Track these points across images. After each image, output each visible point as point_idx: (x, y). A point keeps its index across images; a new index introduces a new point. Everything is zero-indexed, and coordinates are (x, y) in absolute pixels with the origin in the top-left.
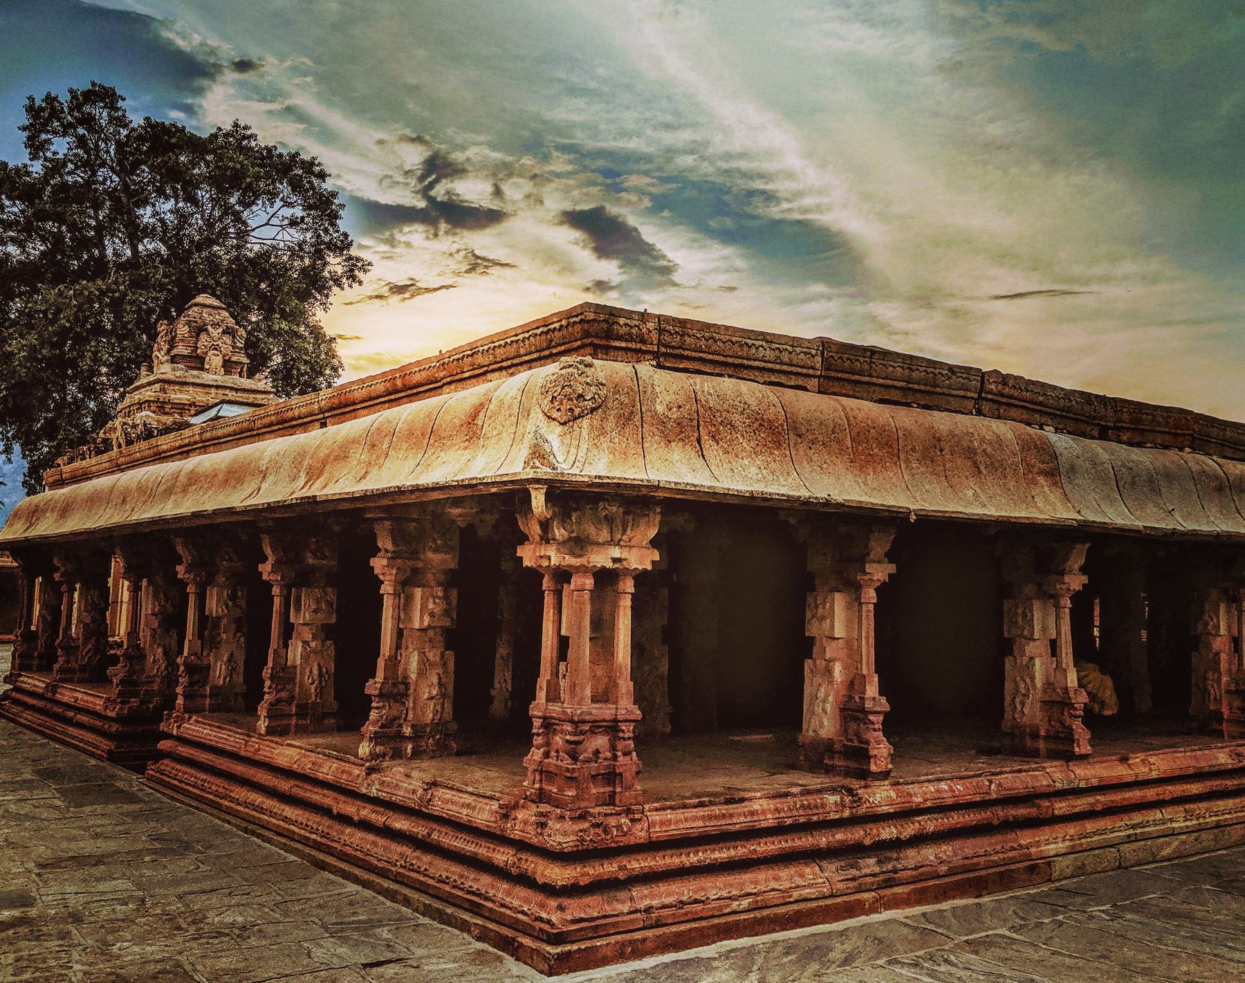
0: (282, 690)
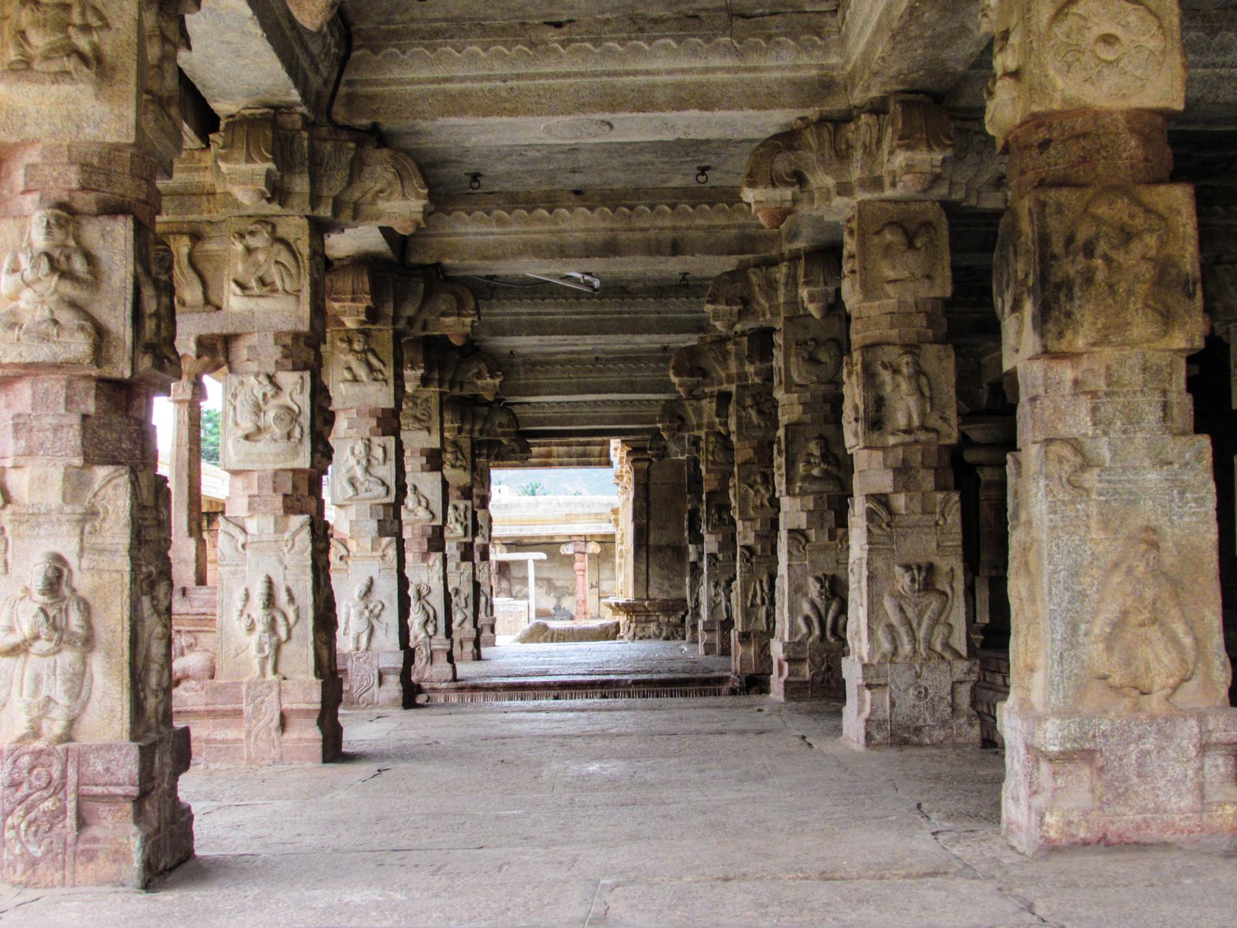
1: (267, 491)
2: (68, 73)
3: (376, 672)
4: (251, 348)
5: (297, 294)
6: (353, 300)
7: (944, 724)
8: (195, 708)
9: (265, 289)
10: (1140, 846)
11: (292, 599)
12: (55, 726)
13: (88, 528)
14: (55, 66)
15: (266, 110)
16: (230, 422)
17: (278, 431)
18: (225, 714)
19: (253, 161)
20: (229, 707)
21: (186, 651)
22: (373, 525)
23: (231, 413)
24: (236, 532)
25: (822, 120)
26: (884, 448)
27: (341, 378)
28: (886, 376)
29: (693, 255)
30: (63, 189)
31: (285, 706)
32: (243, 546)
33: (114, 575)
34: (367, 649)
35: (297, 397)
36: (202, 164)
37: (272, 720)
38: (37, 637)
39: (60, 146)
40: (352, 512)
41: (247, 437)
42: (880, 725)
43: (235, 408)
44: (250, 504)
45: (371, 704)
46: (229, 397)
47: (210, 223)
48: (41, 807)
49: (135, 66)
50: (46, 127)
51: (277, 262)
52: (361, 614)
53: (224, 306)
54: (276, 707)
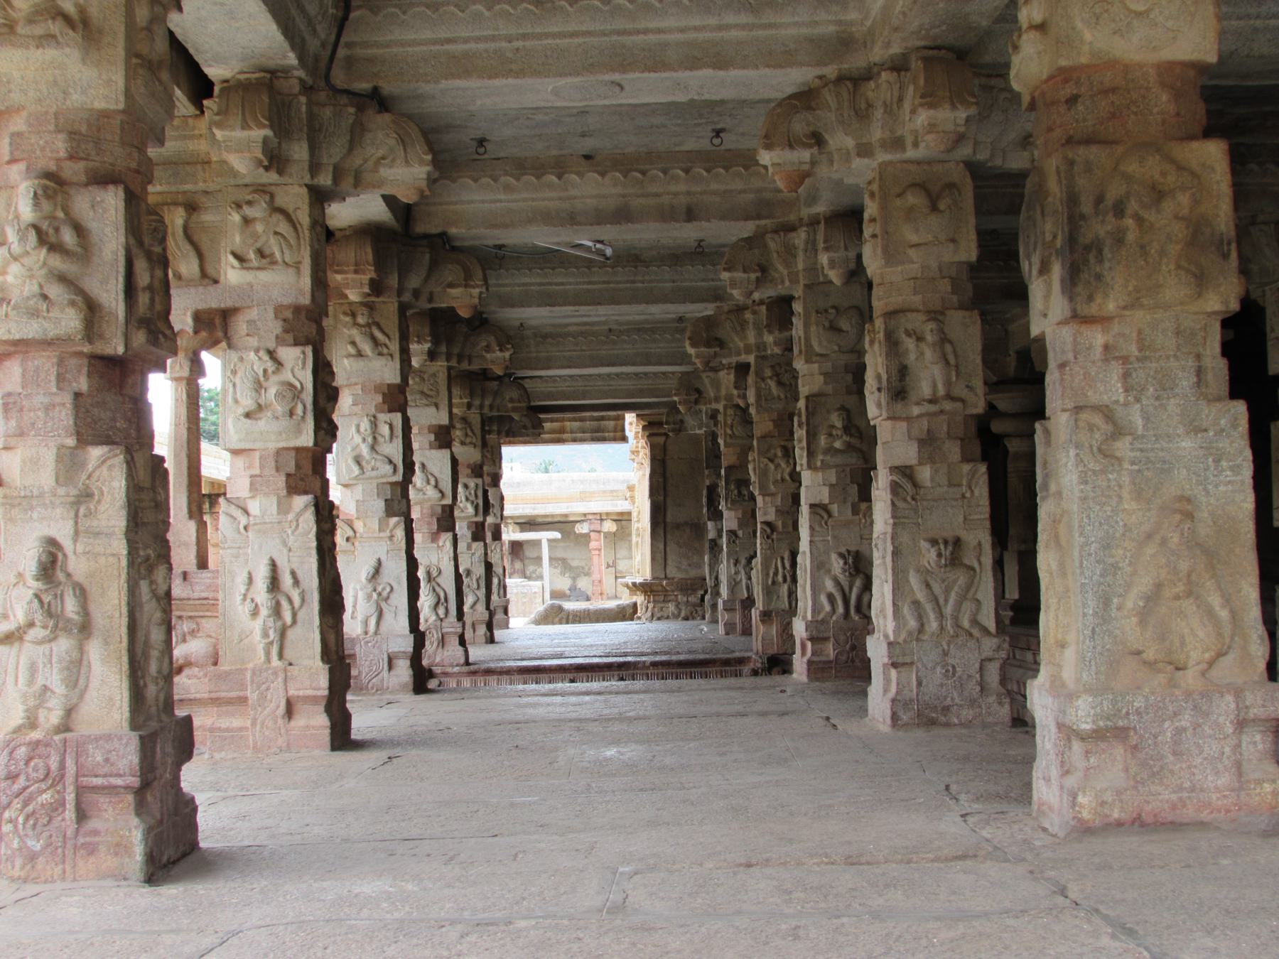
0: (193, 633)
1: (270, 470)
2: (54, 37)
3: (385, 657)
4: (251, 323)
5: (297, 266)
6: (356, 272)
7: (973, 703)
8: (198, 696)
9: (264, 261)
10: (1176, 826)
11: (296, 582)
12: (52, 716)
13: (82, 511)
14: (39, 30)
15: (262, 74)
16: (230, 399)
17: (279, 409)
18: (230, 702)
19: (250, 128)
20: (234, 694)
21: (188, 638)
22: (381, 505)
23: (231, 389)
24: (238, 513)
25: (840, 79)
26: (908, 419)
27: (344, 353)
28: (910, 343)
29: (708, 220)
30: (50, 158)
31: (292, 692)
32: (246, 528)
33: (111, 559)
34: (376, 633)
35: (298, 373)
36: (196, 132)
37: (278, 707)
38: (31, 624)
39: (47, 113)
40: (358, 492)
41: (248, 415)
42: (907, 704)
43: (234, 385)
44: (251, 484)
45: (380, 689)
46: (229, 374)
47: (206, 192)
48: (39, 799)
49: (123, 28)
50: (31, 94)
51: (276, 233)
52: (369, 597)
53: (222, 279)
54: (282, 694)
